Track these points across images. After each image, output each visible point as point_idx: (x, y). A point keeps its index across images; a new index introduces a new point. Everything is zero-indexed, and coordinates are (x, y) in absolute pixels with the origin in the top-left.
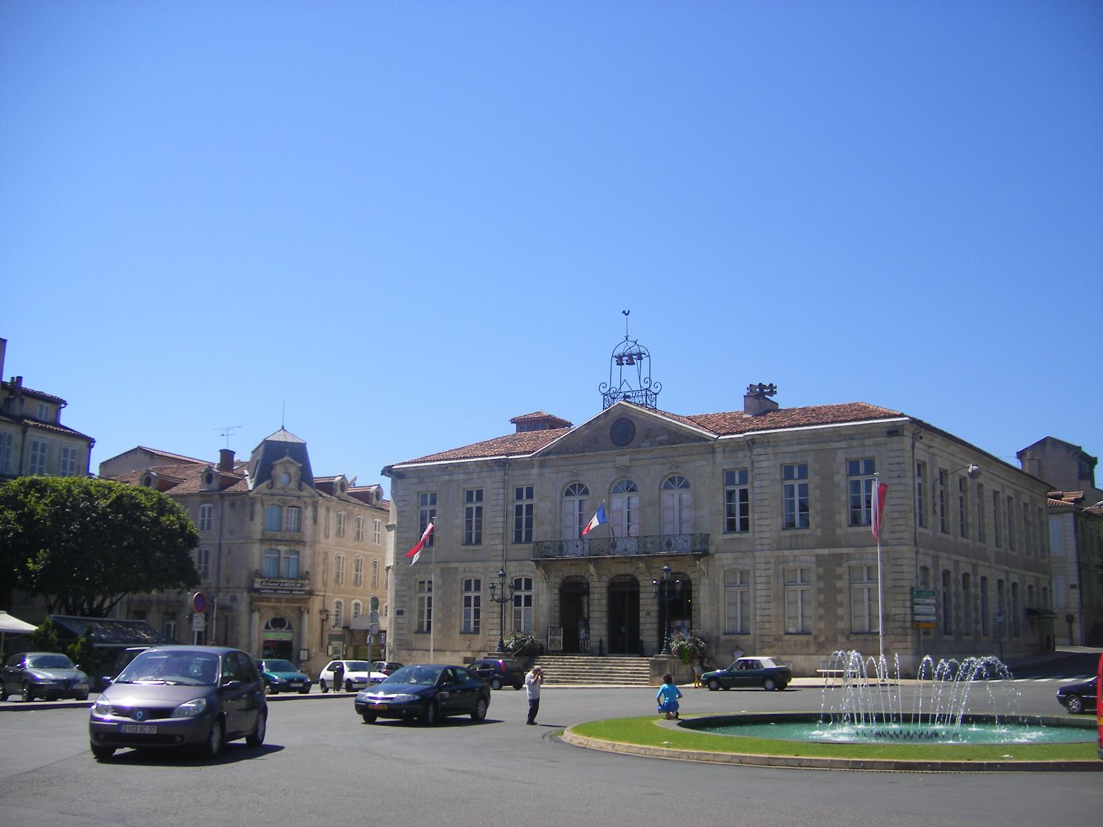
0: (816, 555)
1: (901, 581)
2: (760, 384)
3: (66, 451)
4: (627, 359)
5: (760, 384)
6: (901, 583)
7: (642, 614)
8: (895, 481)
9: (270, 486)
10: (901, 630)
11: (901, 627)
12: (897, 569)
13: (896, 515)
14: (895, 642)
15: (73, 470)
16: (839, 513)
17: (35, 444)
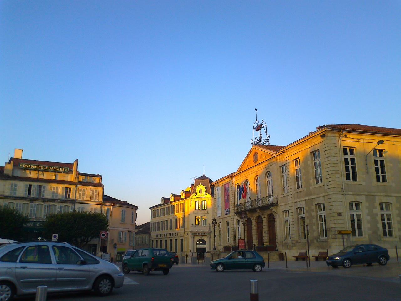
0: (305, 200)
1: (332, 210)
2: (319, 126)
3: (93, 191)
4: (259, 128)
5: (319, 126)
6: (332, 211)
7: (264, 232)
8: (326, 159)
9: (195, 195)
10: (334, 236)
11: (334, 235)
12: (330, 204)
13: (328, 176)
14: (333, 242)
15: (96, 196)
16: (311, 180)
17: (80, 190)
